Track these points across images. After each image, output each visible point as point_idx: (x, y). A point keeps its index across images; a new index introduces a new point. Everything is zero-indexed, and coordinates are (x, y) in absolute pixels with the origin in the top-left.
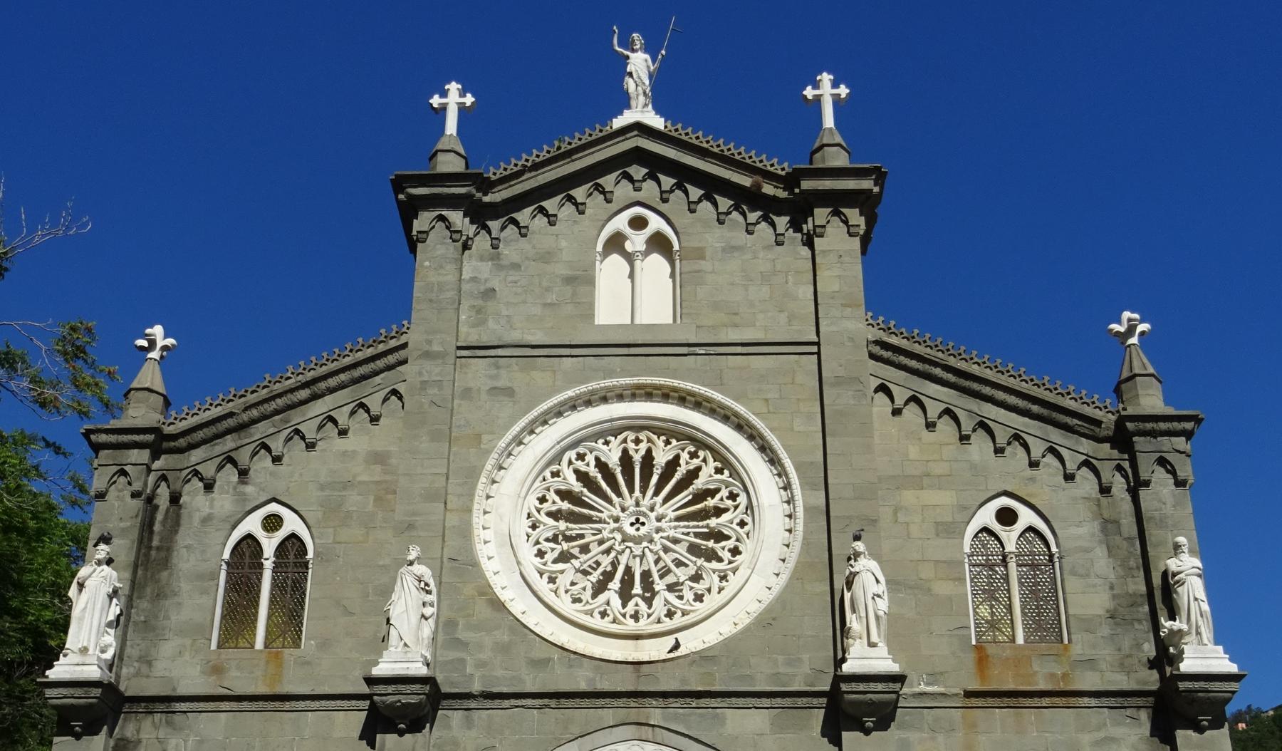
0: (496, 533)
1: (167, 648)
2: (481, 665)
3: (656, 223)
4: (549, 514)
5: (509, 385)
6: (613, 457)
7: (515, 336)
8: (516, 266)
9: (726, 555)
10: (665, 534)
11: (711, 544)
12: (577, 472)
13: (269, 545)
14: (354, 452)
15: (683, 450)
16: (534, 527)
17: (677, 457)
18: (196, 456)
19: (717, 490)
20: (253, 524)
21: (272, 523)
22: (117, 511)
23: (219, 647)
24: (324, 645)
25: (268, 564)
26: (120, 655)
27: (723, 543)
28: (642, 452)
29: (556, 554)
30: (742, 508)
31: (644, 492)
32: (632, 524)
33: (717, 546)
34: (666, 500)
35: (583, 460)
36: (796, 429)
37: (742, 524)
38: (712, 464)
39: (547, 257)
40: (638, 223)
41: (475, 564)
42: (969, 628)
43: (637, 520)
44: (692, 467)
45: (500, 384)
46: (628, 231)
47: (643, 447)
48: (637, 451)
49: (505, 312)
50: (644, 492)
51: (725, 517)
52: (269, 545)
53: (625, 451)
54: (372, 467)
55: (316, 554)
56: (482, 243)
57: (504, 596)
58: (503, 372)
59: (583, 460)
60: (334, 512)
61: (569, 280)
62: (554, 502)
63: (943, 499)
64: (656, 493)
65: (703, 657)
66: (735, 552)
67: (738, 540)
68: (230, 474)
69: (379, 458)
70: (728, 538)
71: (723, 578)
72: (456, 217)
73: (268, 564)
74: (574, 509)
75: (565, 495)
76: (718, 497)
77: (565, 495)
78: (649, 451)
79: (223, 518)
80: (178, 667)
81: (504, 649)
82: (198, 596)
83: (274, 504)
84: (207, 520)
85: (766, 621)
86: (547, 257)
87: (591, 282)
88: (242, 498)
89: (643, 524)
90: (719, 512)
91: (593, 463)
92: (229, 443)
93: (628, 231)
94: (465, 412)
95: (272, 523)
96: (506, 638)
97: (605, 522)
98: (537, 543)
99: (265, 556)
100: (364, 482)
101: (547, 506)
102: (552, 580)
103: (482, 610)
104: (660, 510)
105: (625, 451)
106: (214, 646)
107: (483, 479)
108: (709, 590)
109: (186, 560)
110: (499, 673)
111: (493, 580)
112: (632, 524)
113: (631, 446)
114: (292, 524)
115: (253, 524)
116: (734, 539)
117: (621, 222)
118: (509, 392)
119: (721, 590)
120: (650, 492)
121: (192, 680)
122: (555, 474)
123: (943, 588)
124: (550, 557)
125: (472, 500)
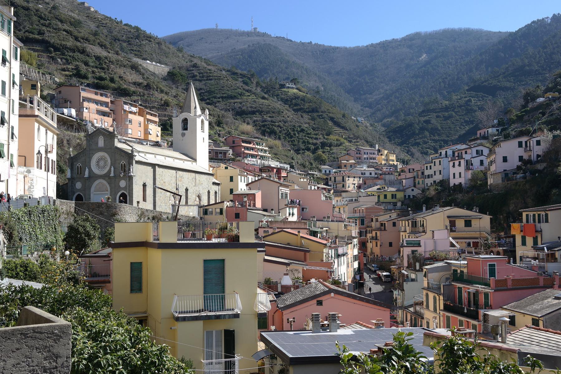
74: (98, 162)
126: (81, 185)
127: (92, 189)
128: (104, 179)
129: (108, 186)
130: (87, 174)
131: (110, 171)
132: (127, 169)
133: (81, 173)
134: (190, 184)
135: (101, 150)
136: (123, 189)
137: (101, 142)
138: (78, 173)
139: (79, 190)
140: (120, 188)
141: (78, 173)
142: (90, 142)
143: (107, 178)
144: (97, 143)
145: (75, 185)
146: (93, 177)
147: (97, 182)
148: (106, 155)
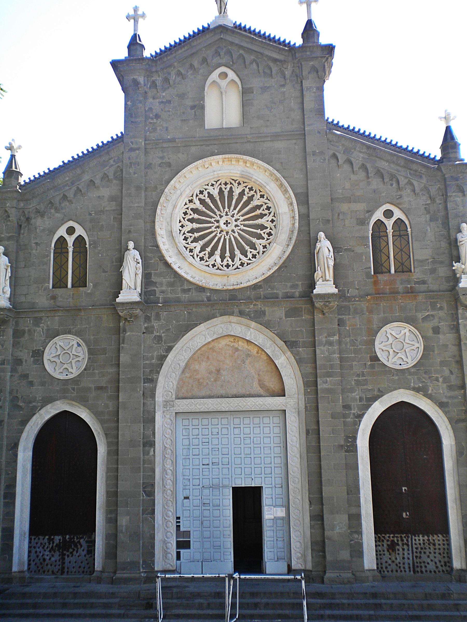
0: (166, 230)
2: (163, 292)
3: (231, 75)
4: (188, 220)
5: (168, 161)
6: (215, 192)
8: (169, 102)
9: (266, 236)
10: (239, 228)
11: (259, 231)
12: (200, 199)
13: (70, 240)
14: (103, 196)
15: (246, 187)
16: (182, 226)
17: (244, 190)
19: (262, 205)
20: (62, 232)
21: (71, 231)
23: (53, 288)
24: (95, 286)
25: (71, 250)
27: (265, 231)
28: (228, 189)
29: (192, 239)
30: (272, 214)
31: (229, 208)
32: (224, 224)
33: (262, 232)
34: (239, 212)
35: (203, 194)
36: (295, 176)
37: (272, 221)
38: (259, 194)
39: (182, 96)
40: (224, 75)
41: (158, 246)
42: (370, 268)
43: (227, 221)
44: (250, 195)
45: (164, 161)
46: (218, 80)
47: (229, 186)
48: (226, 189)
49: (165, 125)
50: (229, 208)
51: (265, 218)
52: (70, 240)
53: (221, 189)
54: (111, 203)
55: (90, 245)
57: (169, 260)
58: (165, 154)
59: (203, 194)
61: (193, 107)
62: (191, 215)
63: (361, 207)
64: (235, 209)
66: (270, 234)
67: (271, 229)
70: (267, 228)
71: (265, 247)
73: (71, 250)
75: (195, 211)
76: (262, 209)
78: (231, 188)
81: (171, 284)
83: (71, 221)
84: (44, 230)
86: (182, 96)
87: (202, 107)
89: (230, 223)
90: (262, 216)
91: (207, 195)
93: (218, 80)
95: (71, 231)
96: (172, 280)
97: (213, 223)
98: (184, 234)
99: (69, 245)
100: (108, 210)
101: (188, 217)
102: (191, 251)
103: (162, 268)
104: (236, 217)
105: (221, 189)
106: (51, 287)
107: (159, 207)
108: (258, 253)
110: (169, 295)
111: (164, 252)
112: (224, 224)
113: (223, 186)
114: (79, 231)
115: (62, 232)
116: (269, 228)
117: (215, 76)
118: (169, 165)
119: (264, 252)
120: (232, 208)
122: (191, 201)
123: (359, 249)
124: (189, 240)
125: (155, 217)
127: (166, 383)
128: (258, 317)
129: (285, 362)
130: (130, 293)
132: (420, 252)
133: (80, 281)
135: (223, 143)
136: (401, 378)
137: (222, 105)
138: (60, 282)
139: (68, 388)
140: (381, 375)
141: (60, 282)
143: (277, 313)
144: (199, 108)
146: (177, 305)
147: (200, 336)
148: (260, 174)
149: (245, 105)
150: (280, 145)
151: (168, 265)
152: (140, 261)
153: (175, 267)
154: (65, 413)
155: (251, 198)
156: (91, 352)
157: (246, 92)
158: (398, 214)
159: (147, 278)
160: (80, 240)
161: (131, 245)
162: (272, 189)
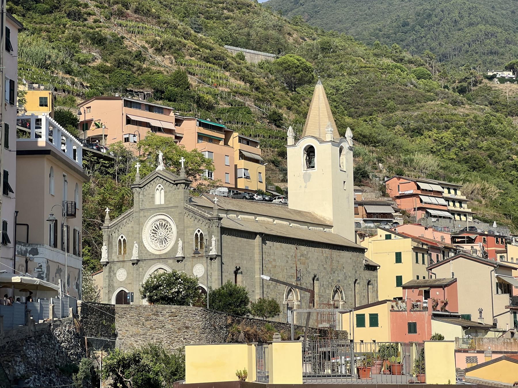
1: (113, 255)
3: (162, 187)
7: (146, 207)
18: (113, 228)
21: (122, 237)
22: (105, 237)
26: (108, 257)
56: (141, 192)
57: (146, 246)
60: (128, 235)
61: (152, 198)
65: (166, 254)
68: (117, 231)
69: (132, 227)
72: (137, 189)
74: (155, 232)
77: (154, 230)
79: (117, 237)
80: (115, 258)
81: (146, 253)
82: (116, 249)
85: (173, 248)
86: (149, 194)
87: (154, 198)
88: (118, 234)
92: (116, 226)
94: (141, 219)
95: (122, 237)
109: (114, 244)
111: (145, 244)
118: (145, 216)
121: (116, 260)
123: (191, 242)
126: (126, 273)
131: (175, 249)
134: (321, 268)
141: (120, 252)
142: (141, 196)
144: (153, 197)
145: (115, 274)
149: (165, 196)
150: (173, 210)
151: (145, 248)
152: (137, 246)
153: (147, 248)
154: (122, 290)
155: (167, 226)
156: (128, 273)
157: (165, 192)
158: (201, 231)
159: (140, 252)
160: (124, 240)
161: (135, 242)
162: (171, 223)
